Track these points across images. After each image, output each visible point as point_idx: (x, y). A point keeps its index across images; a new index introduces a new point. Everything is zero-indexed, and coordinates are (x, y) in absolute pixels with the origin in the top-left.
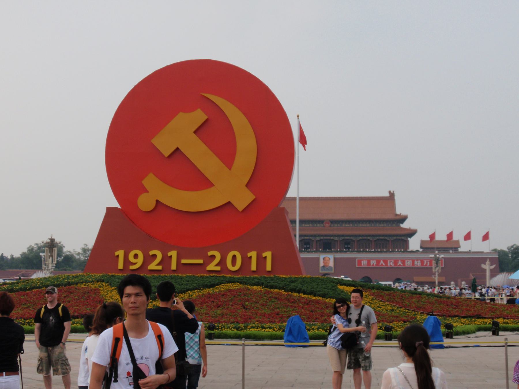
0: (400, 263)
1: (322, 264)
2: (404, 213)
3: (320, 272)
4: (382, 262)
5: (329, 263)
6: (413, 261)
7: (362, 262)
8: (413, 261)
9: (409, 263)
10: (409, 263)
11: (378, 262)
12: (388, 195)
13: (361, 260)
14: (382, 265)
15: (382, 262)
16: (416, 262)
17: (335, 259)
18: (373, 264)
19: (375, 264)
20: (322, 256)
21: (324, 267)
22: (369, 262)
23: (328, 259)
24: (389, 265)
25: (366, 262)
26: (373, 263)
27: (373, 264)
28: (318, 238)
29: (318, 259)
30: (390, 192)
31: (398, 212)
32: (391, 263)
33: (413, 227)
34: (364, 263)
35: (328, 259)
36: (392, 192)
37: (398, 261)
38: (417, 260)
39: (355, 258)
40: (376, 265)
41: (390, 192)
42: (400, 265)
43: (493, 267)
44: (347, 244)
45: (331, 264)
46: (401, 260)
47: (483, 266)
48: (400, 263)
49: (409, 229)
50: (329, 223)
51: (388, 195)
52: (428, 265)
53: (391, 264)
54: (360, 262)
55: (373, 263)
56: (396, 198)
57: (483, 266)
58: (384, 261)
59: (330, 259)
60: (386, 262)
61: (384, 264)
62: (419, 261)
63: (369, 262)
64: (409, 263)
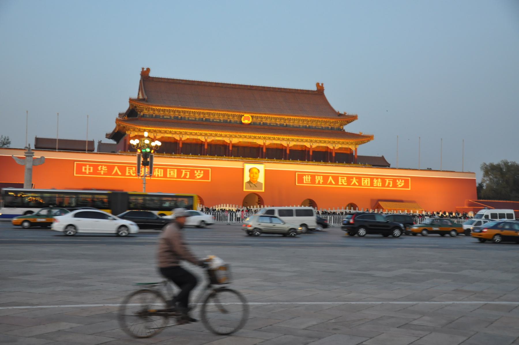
0: (354, 181)
1: (247, 178)
2: (350, 112)
3: (244, 190)
4: (330, 178)
5: (257, 178)
6: (372, 180)
7: (304, 177)
9: (366, 181)
11: (326, 178)
13: (303, 175)
14: (331, 182)
15: (330, 178)
16: (375, 181)
18: (319, 181)
19: (321, 181)
20: (248, 167)
21: (249, 182)
23: (256, 171)
24: (340, 183)
25: (310, 178)
27: (319, 181)
29: (243, 169)
30: (318, 85)
32: (343, 181)
34: (307, 179)
35: (256, 171)
36: (320, 85)
37: (352, 178)
38: (377, 179)
39: (296, 172)
40: (323, 183)
42: (355, 185)
45: (261, 179)
46: (356, 178)
48: (354, 181)
50: (249, 120)
51: (314, 88)
52: (391, 186)
54: (301, 178)
55: (319, 179)
56: (326, 93)
58: (333, 177)
59: (259, 170)
60: (336, 179)
61: (334, 183)
62: (379, 180)
64: (366, 181)
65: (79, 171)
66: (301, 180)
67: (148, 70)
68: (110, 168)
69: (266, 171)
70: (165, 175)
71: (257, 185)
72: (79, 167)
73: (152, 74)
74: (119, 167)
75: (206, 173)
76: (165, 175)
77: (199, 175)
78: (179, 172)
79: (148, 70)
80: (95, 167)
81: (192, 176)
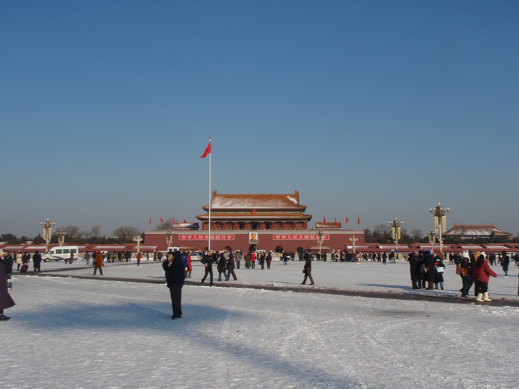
0: (301, 237)
1: (250, 238)
2: (304, 205)
6: (309, 236)
8: (309, 236)
10: (307, 237)
11: (287, 236)
12: (294, 193)
17: (259, 235)
20: (250, 233)
21: (251, 240)
22: (281, 236)
26: (284, 237)
28: (248, 221)
30: (295, 191)
31: (300, 204)
33: (310, 214)
34: (278, 237)
41: (295, 191)
43: (357, 240)
44: (268, 225)
45: (257, 238)
47: (351, 239)
48: (301, 237)
49: (307, 215)
51: (294, 193)
53: (295, 238)
55: (284, 237)
57: (351, 239)
60: (292, 236)
63: (281, 236)
65: (181, 238)
66: (275, 238)
67: (216, 191)
68: (193, 236)
69: (259, 235)
70: (215, 238)
71: (255, 241)
72: (181, 236)
73: (217, 193)
74: (197, 236)
75: (232, 236)
76: (215, 238)
77: (229, 238)
78: (221, 237)
79: (216, 191)
80: (187, 236)
81: (226, 238)
